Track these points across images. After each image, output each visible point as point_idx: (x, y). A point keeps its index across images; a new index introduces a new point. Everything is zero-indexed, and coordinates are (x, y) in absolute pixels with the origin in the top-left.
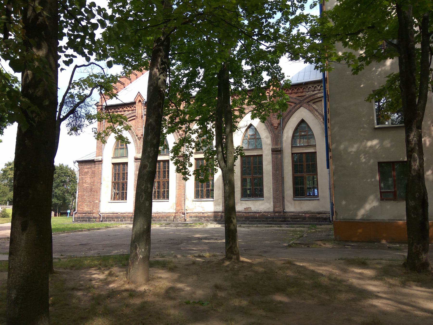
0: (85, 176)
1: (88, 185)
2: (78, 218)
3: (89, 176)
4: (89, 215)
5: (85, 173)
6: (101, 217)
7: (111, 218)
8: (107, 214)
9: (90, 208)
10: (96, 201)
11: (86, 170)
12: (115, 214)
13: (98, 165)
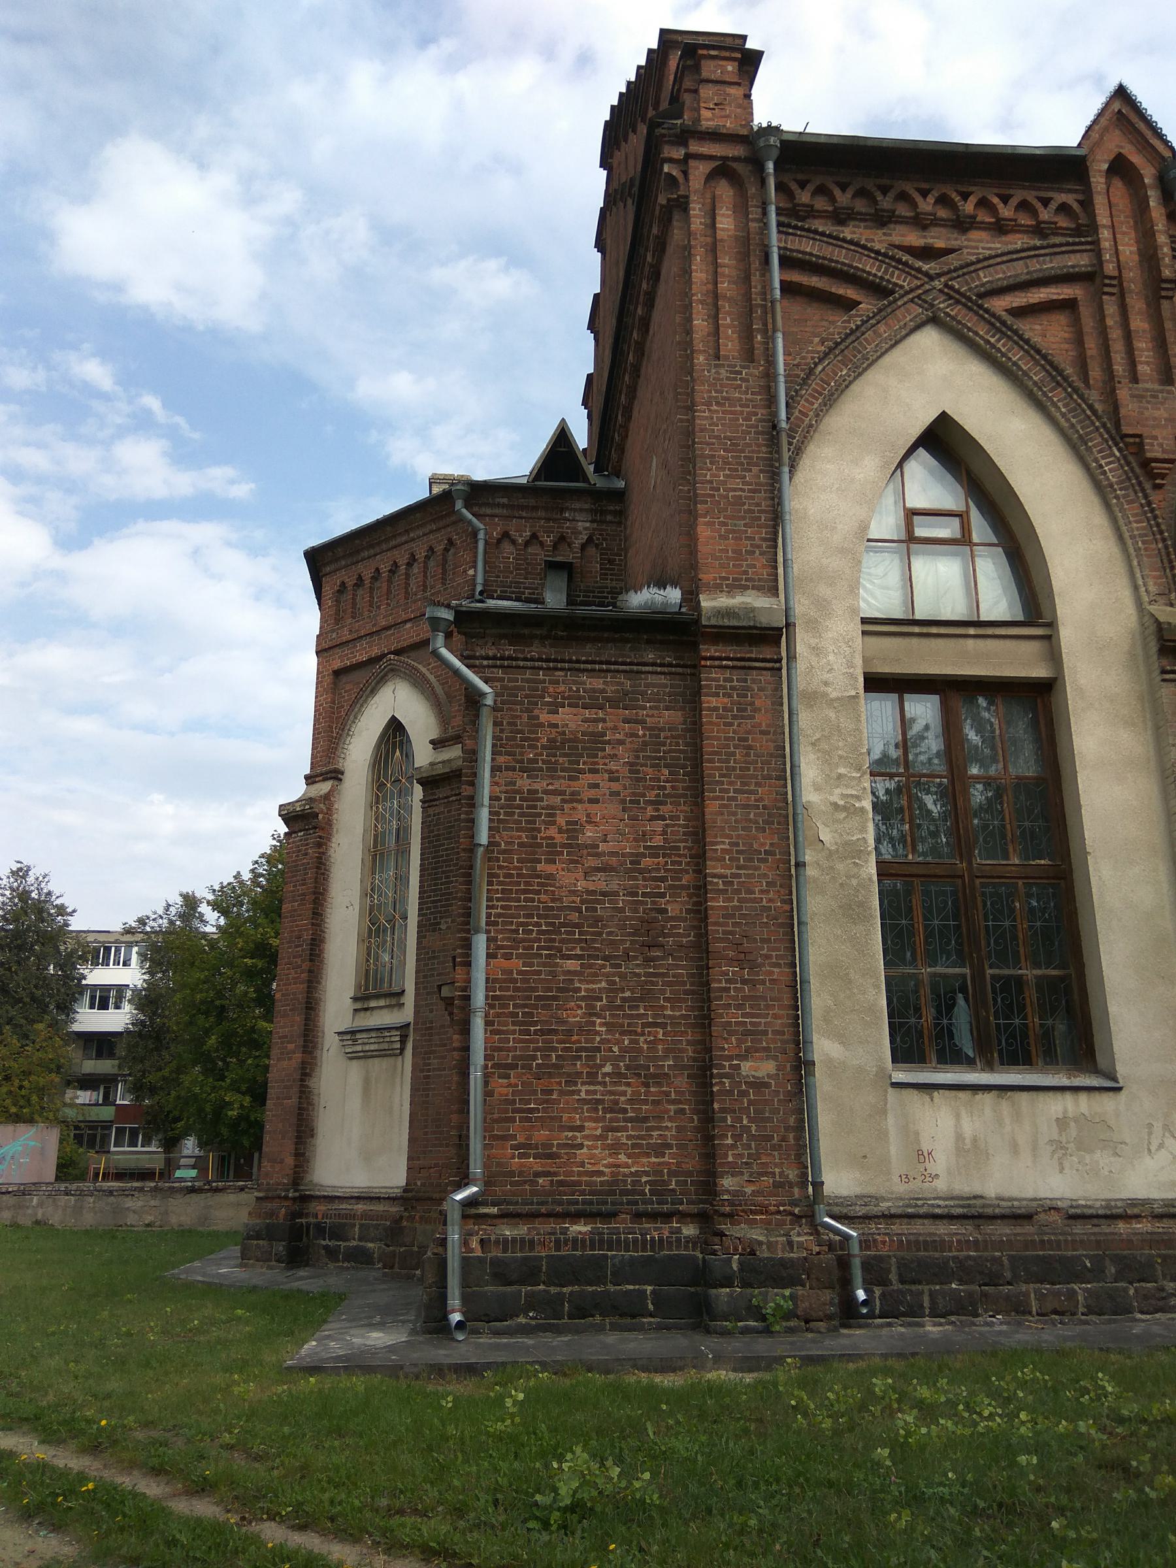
0: (557, 785)
1: (600, 882)
2: (501, 1273)
3: (606, 786)
4: (655, 1231)
5: (552, 745)
6: (857, 1263)
7: (964, 1271)
8: (897, 1227)
9: (659, 1150)
10: (746, 1067)
11: (569, 719)
12: (1003, 1231)
13: (741, 674)
